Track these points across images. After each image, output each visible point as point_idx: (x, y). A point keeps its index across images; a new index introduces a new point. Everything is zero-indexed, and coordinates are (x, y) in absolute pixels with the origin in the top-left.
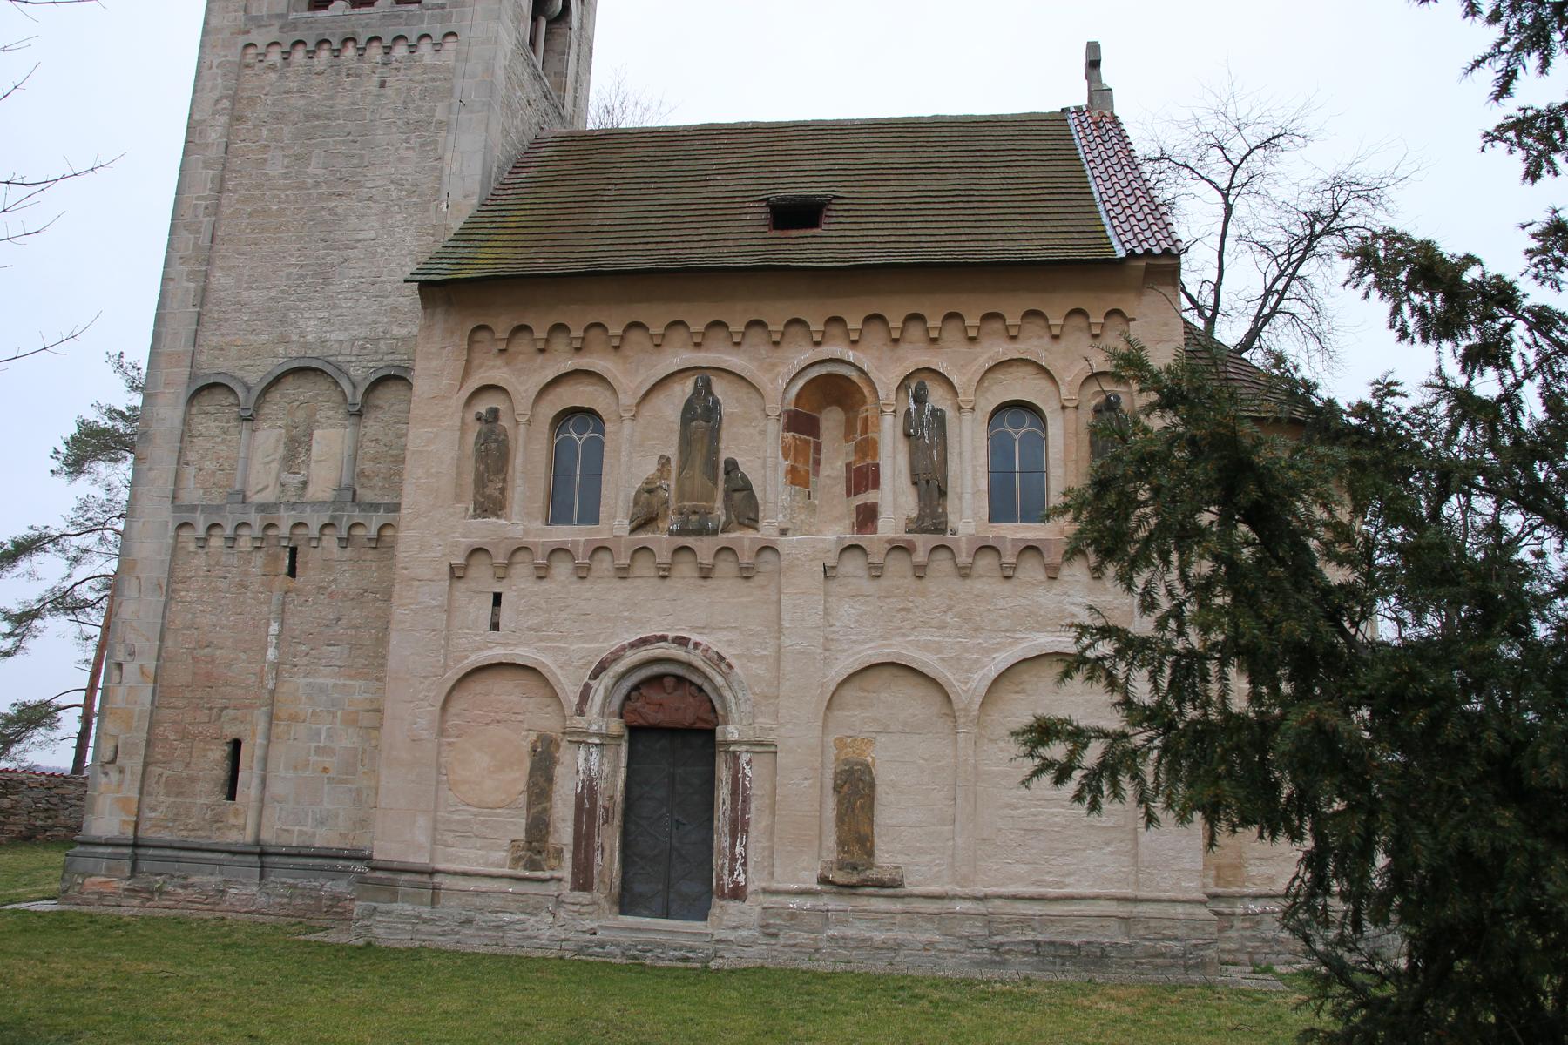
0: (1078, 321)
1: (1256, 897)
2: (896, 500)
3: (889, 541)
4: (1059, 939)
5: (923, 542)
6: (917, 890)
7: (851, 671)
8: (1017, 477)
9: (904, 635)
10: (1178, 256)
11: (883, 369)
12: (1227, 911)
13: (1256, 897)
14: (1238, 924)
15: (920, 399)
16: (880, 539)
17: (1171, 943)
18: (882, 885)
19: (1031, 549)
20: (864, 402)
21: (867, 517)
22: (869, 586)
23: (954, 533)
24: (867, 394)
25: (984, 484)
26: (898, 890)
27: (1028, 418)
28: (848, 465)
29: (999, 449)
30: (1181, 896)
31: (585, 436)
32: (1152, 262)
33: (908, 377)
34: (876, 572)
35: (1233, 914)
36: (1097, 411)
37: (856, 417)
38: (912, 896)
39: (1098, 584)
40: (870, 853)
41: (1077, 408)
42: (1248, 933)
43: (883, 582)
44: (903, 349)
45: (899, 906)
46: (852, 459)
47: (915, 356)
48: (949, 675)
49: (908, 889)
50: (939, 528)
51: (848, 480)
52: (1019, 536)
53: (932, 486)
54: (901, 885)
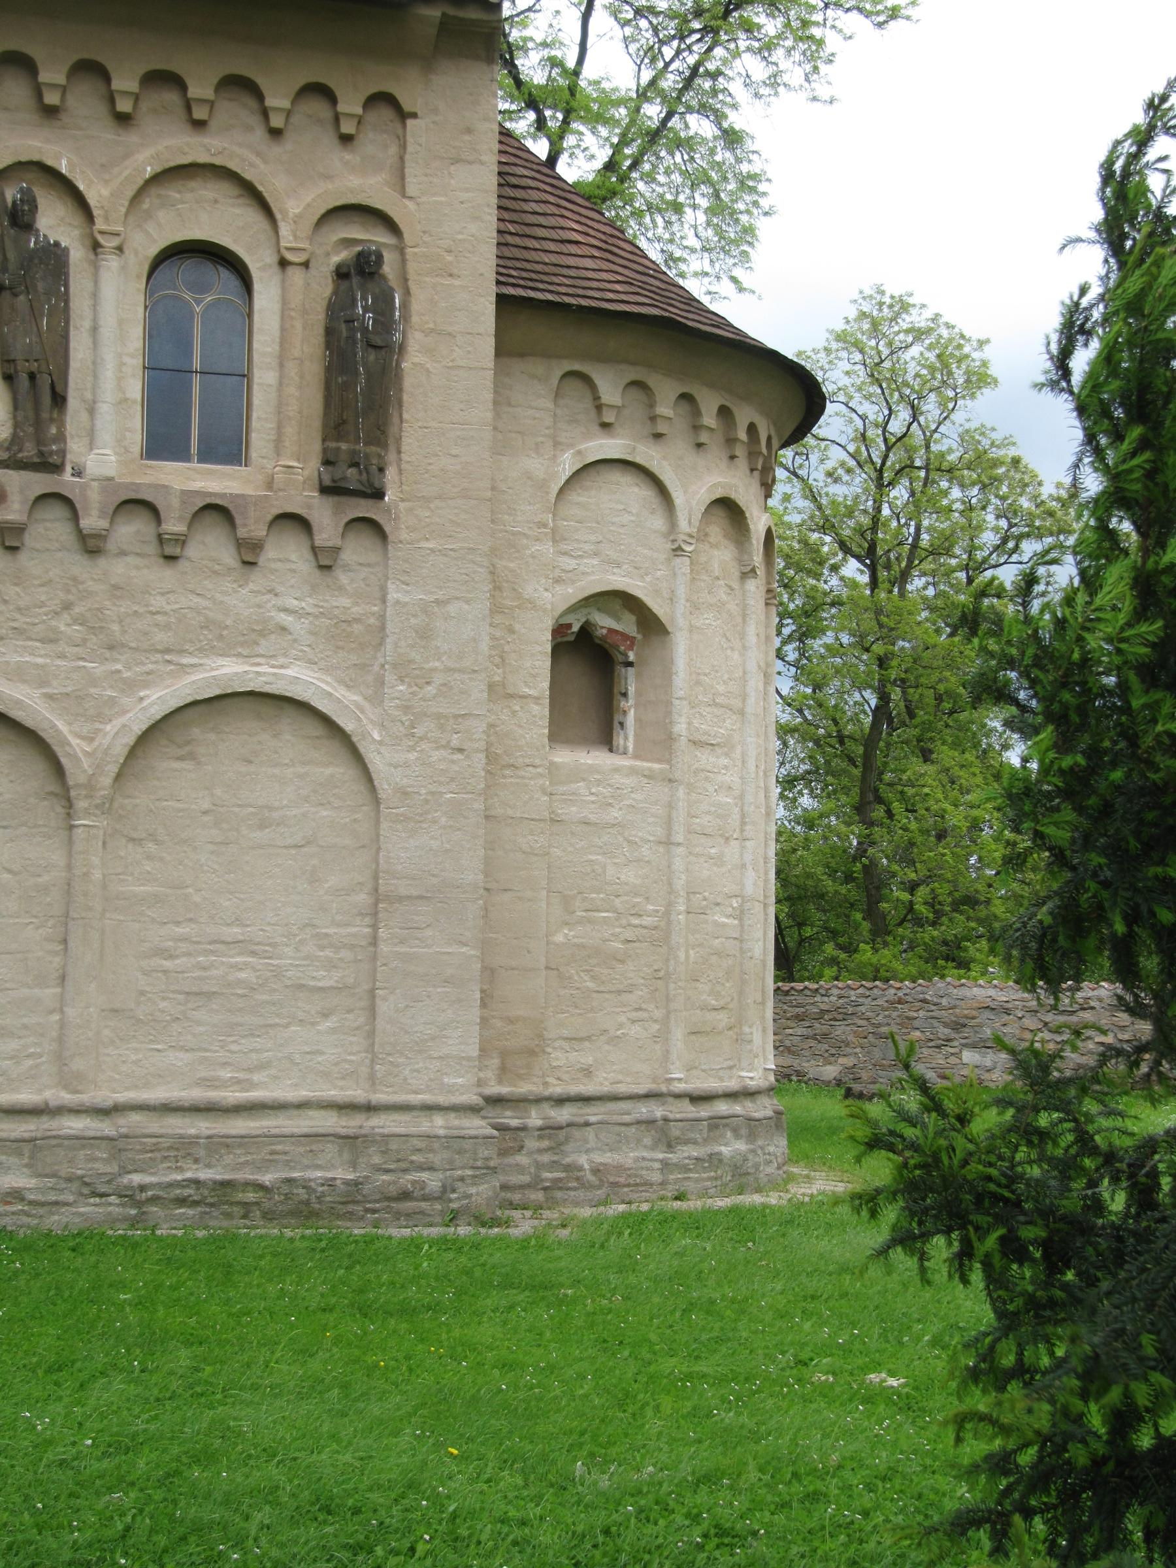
0: (317, 107)
4: (239, 1176)
8: (196, 380)
12: (514, 1123)
13: (561, 1101)
14: (531, 1144)
17: (424, 1176)
19: (217, 511)
23: (78, 473)
25: (135, 389)
30: (441, 1099)
35: (524, 1128)
36: (341, 274)
41: (306, 265)
42: (546, 1158)
50: (49, 465)
52: (198, 485)
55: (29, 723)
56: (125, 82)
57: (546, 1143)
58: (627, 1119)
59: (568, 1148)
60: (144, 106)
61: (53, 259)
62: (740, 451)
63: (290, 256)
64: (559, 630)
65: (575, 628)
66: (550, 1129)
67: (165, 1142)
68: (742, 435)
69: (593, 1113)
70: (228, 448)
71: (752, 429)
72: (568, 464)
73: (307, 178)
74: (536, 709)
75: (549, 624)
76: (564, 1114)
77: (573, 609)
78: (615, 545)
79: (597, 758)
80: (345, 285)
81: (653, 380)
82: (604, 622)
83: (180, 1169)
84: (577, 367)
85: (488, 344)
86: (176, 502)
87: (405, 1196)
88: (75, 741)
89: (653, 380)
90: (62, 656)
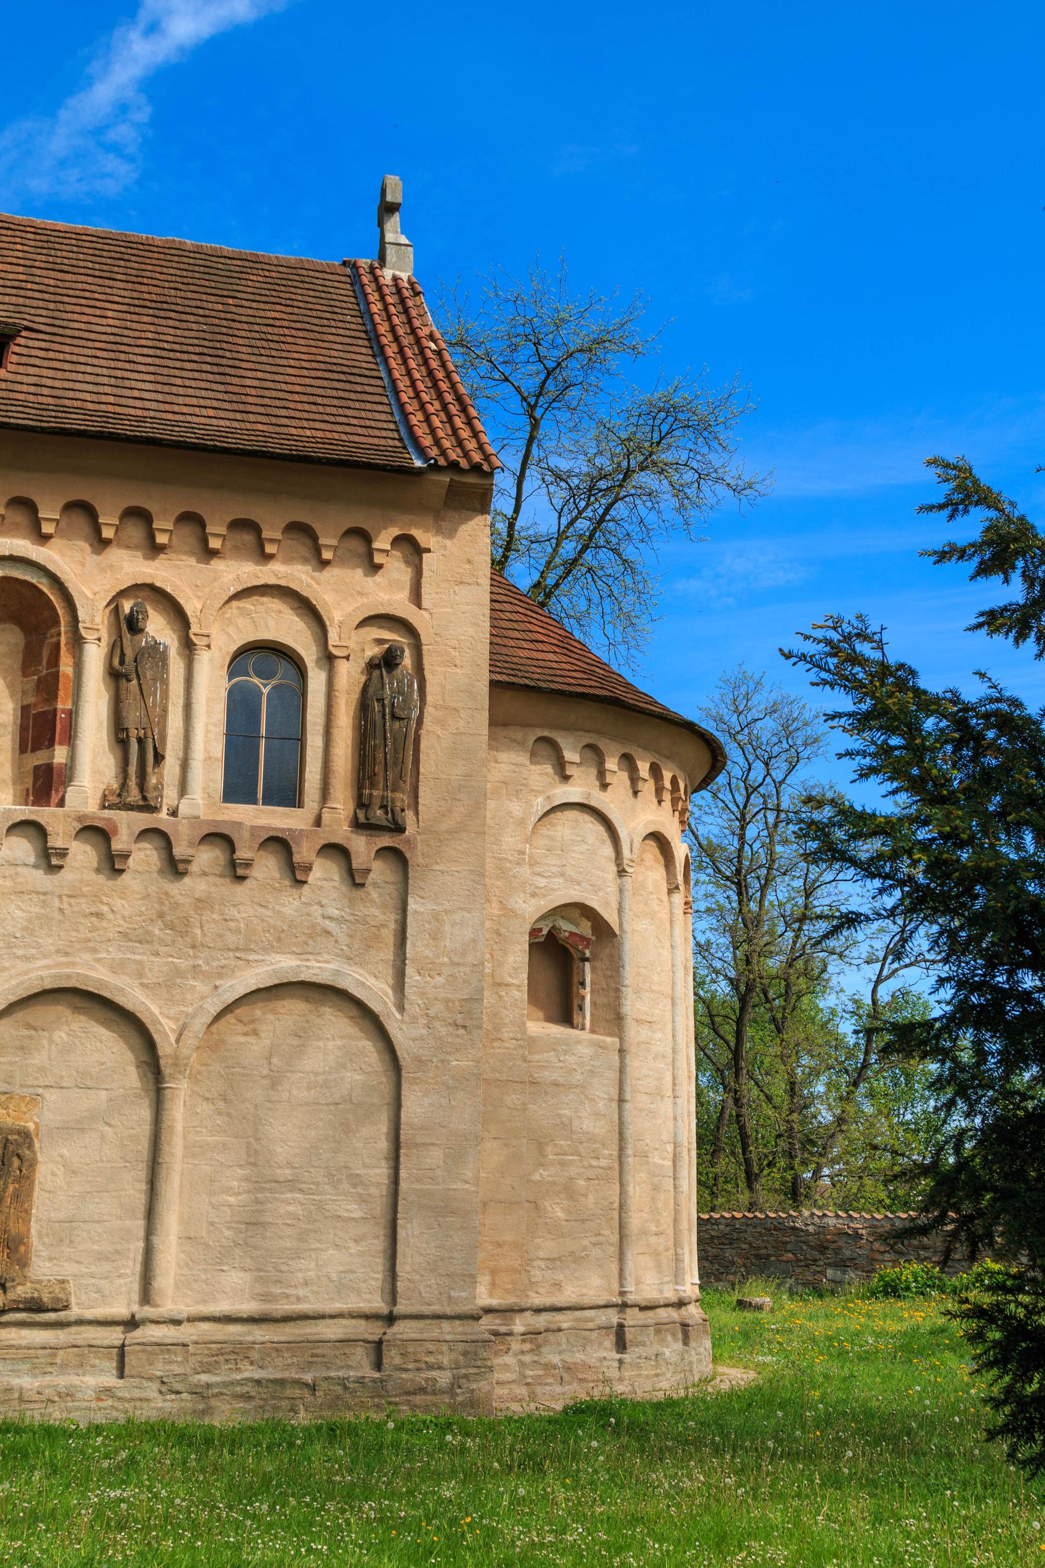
0: (356, 544)
1: (538, 1311)
2: (93, 762)
3: (79, 819)
4: (286, 1375)
5: (127, 824)
6: (89, 1314)
7: (13, 998)
8: (263, 742)
9: (95, 951)
10: (491, 475)
11: (91, 576)
12: (503, 1329)
13: (538, 1311)
14: (515, 1346)
15: (134, 625)
16: (67, 816)
17: (434, 1374)
18: (35, 1306)
19: (279, 843)
20: (57, 623)
21: (45, 784)
22: (39, 878)
23: (174, 813)
24: (60, 612)
25: (218, 749)
26: (62, 1315)
27: (283, 667)
28: (25, 710)
29: (241, 709)
30: (448, 1311)
31: (274, 682)
32: (457, 478)
33: (122, 594)
34: (50, 859)
35: (510, 1334)
36: (372, 666)
37: (42, 642)
38: (81, 1322)
39: (360, 893)
40: (24, 1263)
41: (347, 658)
42: (527, 1358)
43: (66, 876)
44: (115, 555)
45: (59, 1337)
46: (31, 700)
47: (130, 566)
48: (156, 1010)
49: (75, 1312)
50: (148, 807)
51: (23, 729)
52: (263, 822)
53: (138, 748)
54: (66, 1307)
55: (129, 1006)
56: (216, 527)
57: (527, 1346)
58: (591, 1325)
59: (543, 1350)
60: (228, 544)
61: (156, 653)
62: (667, 797)
63: (335, 652)
64: (534, 932)
65: (545, 932)
66: (533, 1334)
67: (228, 1348)
68: (667, 784)
69: (565, 1320)
70: (287, 793)
71: (674, 781)
72: (540, 804)
73: (347, 595)
74: (517, 994)
75: (528, 928)
76: (542, 1321)
77: (543, 918)
78: (570, 869)
79: (557, 1030)
80: (376, 673)
81: (602, 743)
82: (566, 927)
83: (239, 1370)
84: (546, 733)
85: (483, 717)
86: (246, 835)
87: (422, 1390)
88: (164, 1021)
89: (602, 743)
90: (157, 954)
